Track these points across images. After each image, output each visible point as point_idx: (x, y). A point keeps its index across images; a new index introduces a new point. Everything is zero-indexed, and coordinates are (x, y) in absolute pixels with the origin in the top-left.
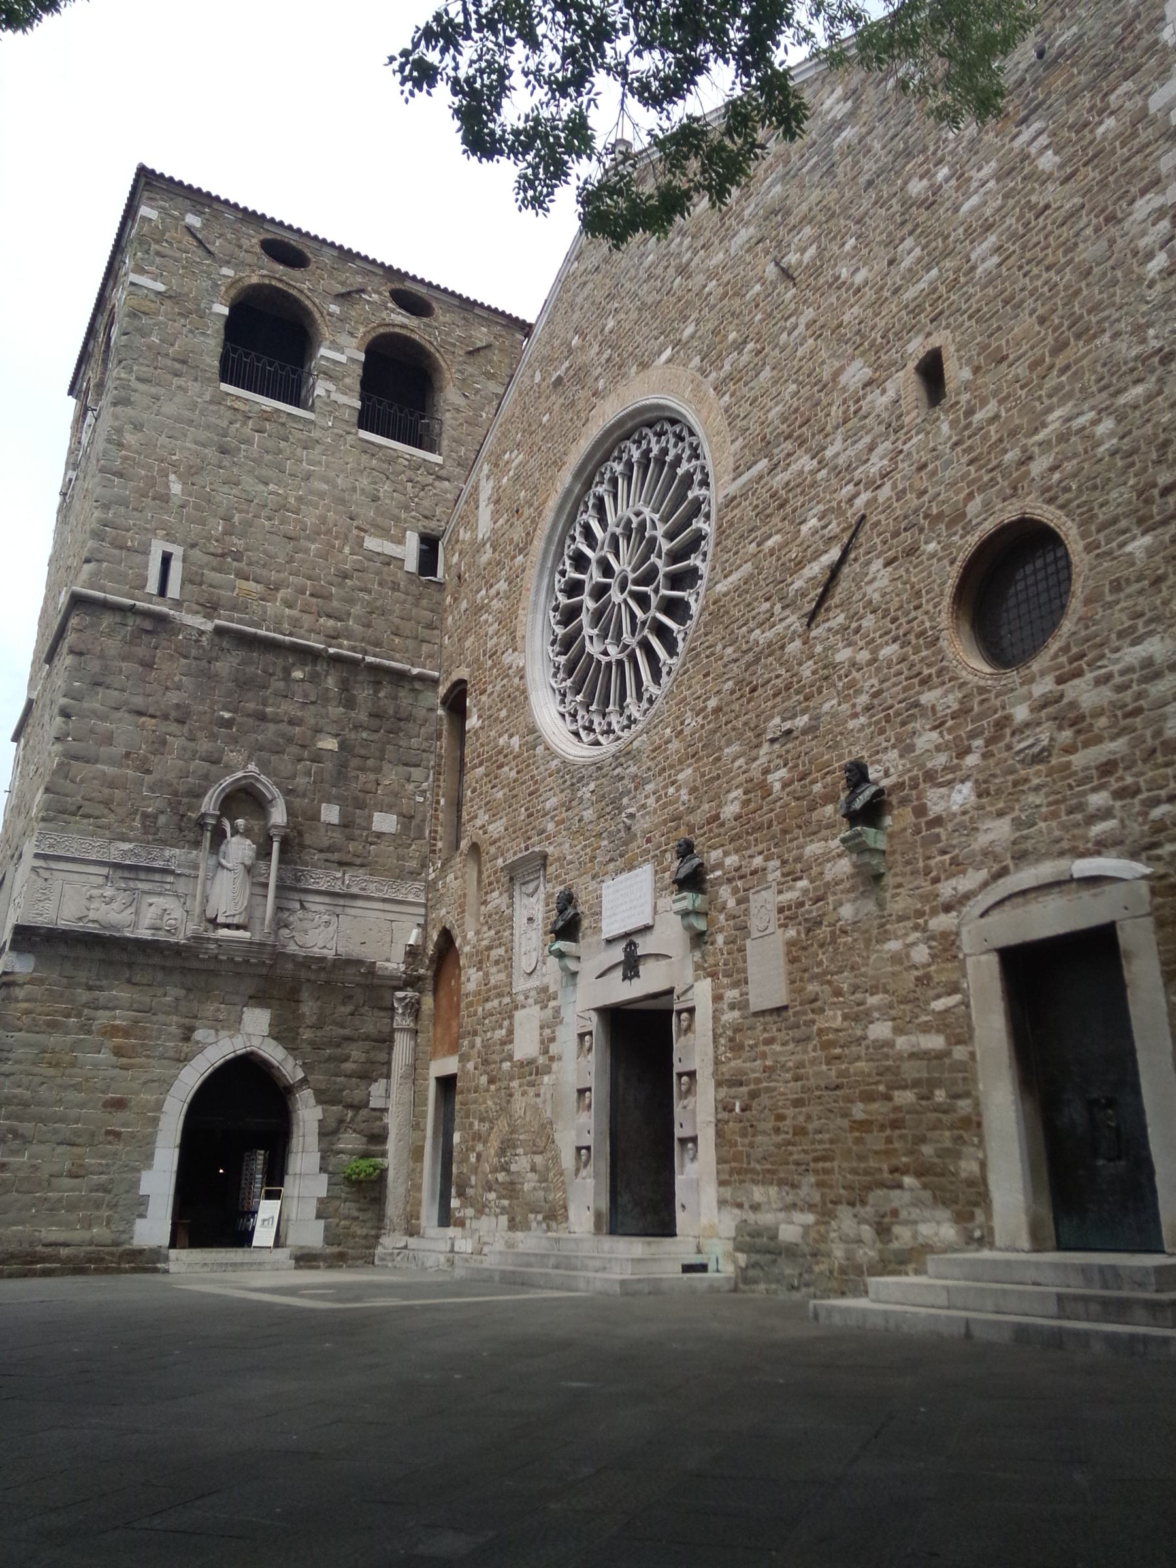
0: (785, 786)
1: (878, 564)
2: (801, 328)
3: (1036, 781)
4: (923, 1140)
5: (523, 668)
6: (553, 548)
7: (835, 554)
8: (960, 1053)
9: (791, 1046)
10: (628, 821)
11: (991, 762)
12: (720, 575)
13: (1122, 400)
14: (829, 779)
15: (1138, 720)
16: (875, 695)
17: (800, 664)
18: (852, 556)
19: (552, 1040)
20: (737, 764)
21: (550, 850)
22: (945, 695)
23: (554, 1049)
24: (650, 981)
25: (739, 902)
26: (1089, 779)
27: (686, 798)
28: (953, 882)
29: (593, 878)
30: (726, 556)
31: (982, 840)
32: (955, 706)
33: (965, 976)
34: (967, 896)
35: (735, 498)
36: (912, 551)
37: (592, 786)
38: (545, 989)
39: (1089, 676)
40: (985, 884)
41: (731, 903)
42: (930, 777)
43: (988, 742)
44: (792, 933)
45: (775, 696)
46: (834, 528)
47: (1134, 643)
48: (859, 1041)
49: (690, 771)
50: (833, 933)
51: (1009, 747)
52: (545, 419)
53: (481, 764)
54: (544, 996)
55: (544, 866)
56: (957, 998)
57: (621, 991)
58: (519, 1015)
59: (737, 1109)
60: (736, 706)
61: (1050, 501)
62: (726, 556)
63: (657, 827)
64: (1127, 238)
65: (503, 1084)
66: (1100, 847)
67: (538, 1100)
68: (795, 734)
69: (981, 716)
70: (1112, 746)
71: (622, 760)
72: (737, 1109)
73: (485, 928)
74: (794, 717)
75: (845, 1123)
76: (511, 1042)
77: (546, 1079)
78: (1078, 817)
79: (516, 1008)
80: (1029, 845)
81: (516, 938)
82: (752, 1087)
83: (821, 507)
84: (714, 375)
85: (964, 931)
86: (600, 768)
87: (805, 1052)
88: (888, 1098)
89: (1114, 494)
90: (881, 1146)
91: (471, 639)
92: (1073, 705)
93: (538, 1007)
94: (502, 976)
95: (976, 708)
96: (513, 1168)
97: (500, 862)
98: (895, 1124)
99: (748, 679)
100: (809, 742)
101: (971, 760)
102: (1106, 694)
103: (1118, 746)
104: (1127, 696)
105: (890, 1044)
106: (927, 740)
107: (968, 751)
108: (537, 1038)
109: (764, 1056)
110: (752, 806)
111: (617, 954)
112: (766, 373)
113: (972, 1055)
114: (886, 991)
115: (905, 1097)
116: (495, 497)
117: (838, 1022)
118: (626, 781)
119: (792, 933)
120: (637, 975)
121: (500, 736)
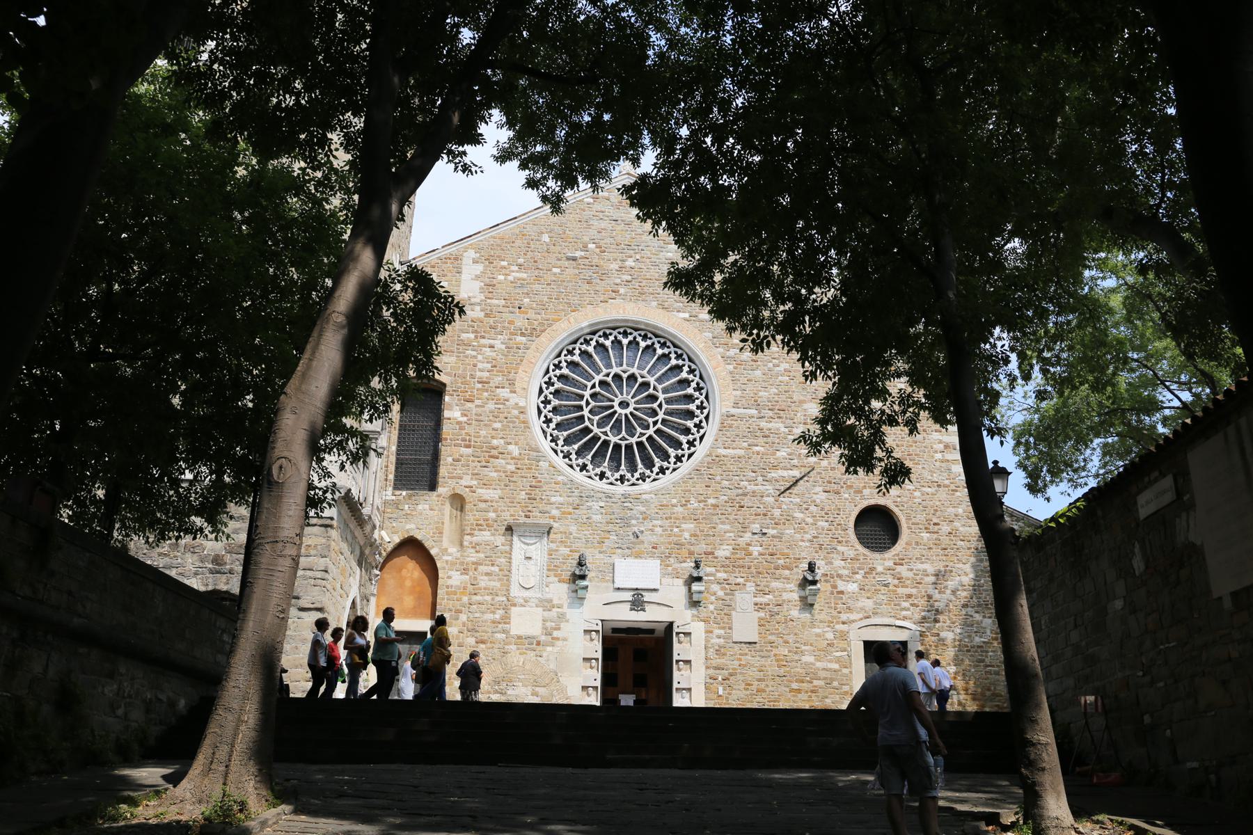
0: (761, 554)
1: (821, 489)
2: (781, 368)
3: (883, 592)
4: (827, 697)
5: (524, 408)
6: (557, 351)
7: (796, 473)
8: (845, 671)
9: (758, 658)
10: (639, 534)
11: (867, 580)
12: (720, 445)
13: (924, 489)
14: (788, 560)
15: (920, 586)
16: (814, 537)
17: (773, 508)
18: (806, 478)
19: (559, 629)
20: (728, 534)
21: (555, 525)
22: (849, 550)
23: (555, 634)
24: (651, 615)
25: (726, 594)
26: (903, 597)
27: (688, 537)
28: (848, 615)
29: (600, 552)
30: (725, 439)
31: (860, 604)
32: (852, 556)
33: (849, 645)
34: (853, 621)
35: (734, 416)
36: (837, 493)
37: (602, 504)
38: (551, 601)
39: (905, 567)
40: (861, 619)
41: (721, 593)
42: (840, 576)
43: (865, 573)
44: (762, 614)
45: (756, 515)
46: (795, 462)
47: (922, 563)
48: (797, 661)
49: (692, 526)
50: (786, 620)
51: (874, 578)
52: (555, 270)
53: (468, 446)
54: (547, 604)
55: (549, 533)
56: (846, 653)
57: (625, 615)
58: (513, 608)
59: (720, 679)
60: (730, 509)
61: (897, 506)
62: (725, 439)
63: (662, 543)
64: (929, 441)
65: (496, 646)
66: (905, 618)
67: (539, 659)
68: (768, 535)
69: (863, 563)
70: (912, 590)
71: (632, 500)
72: (720, 679)
73: (473, 551)
74: (768, 528)
75: (788, 689)
76: (509, 623)
77: (549, 649)
78: (898, 607)
79: (515, 605)
80: (879, 611)
81: (513, 565)
82: (731, 671)
83: (789, 450)
84: (721, 350)
85: (851, 633)
86: (610, 497)
87: (766, 661)
88: (812, 683)
89: (918, 516)
90: (806, 698)
91: (453, 359)
92: (899, 573)
93: (541, 609)
94: (498, 584)
95: (862, 561)
96: (509, 692)
97: (492, 515)
98: (812, 691)
99: (738, 501)
100: (776, 541)
101: (859, 577)
102: (910, 574)
103: (914, 591)
104: (918, 578)
105: (814, 664)
106: (838, 563)
107: (857, 573)
108: (540, 624)
109: (740, 660)
110: (738, 556)
111: (628, 596)
112: (758, 373)
113: (851, 672)
114: (811, 645)
115: (821, 683)
116: (488, 280)
117: (786, 653)
118: (635, 512)
119: (762, 614)
120: (643, 610)
121: (493, 437)
